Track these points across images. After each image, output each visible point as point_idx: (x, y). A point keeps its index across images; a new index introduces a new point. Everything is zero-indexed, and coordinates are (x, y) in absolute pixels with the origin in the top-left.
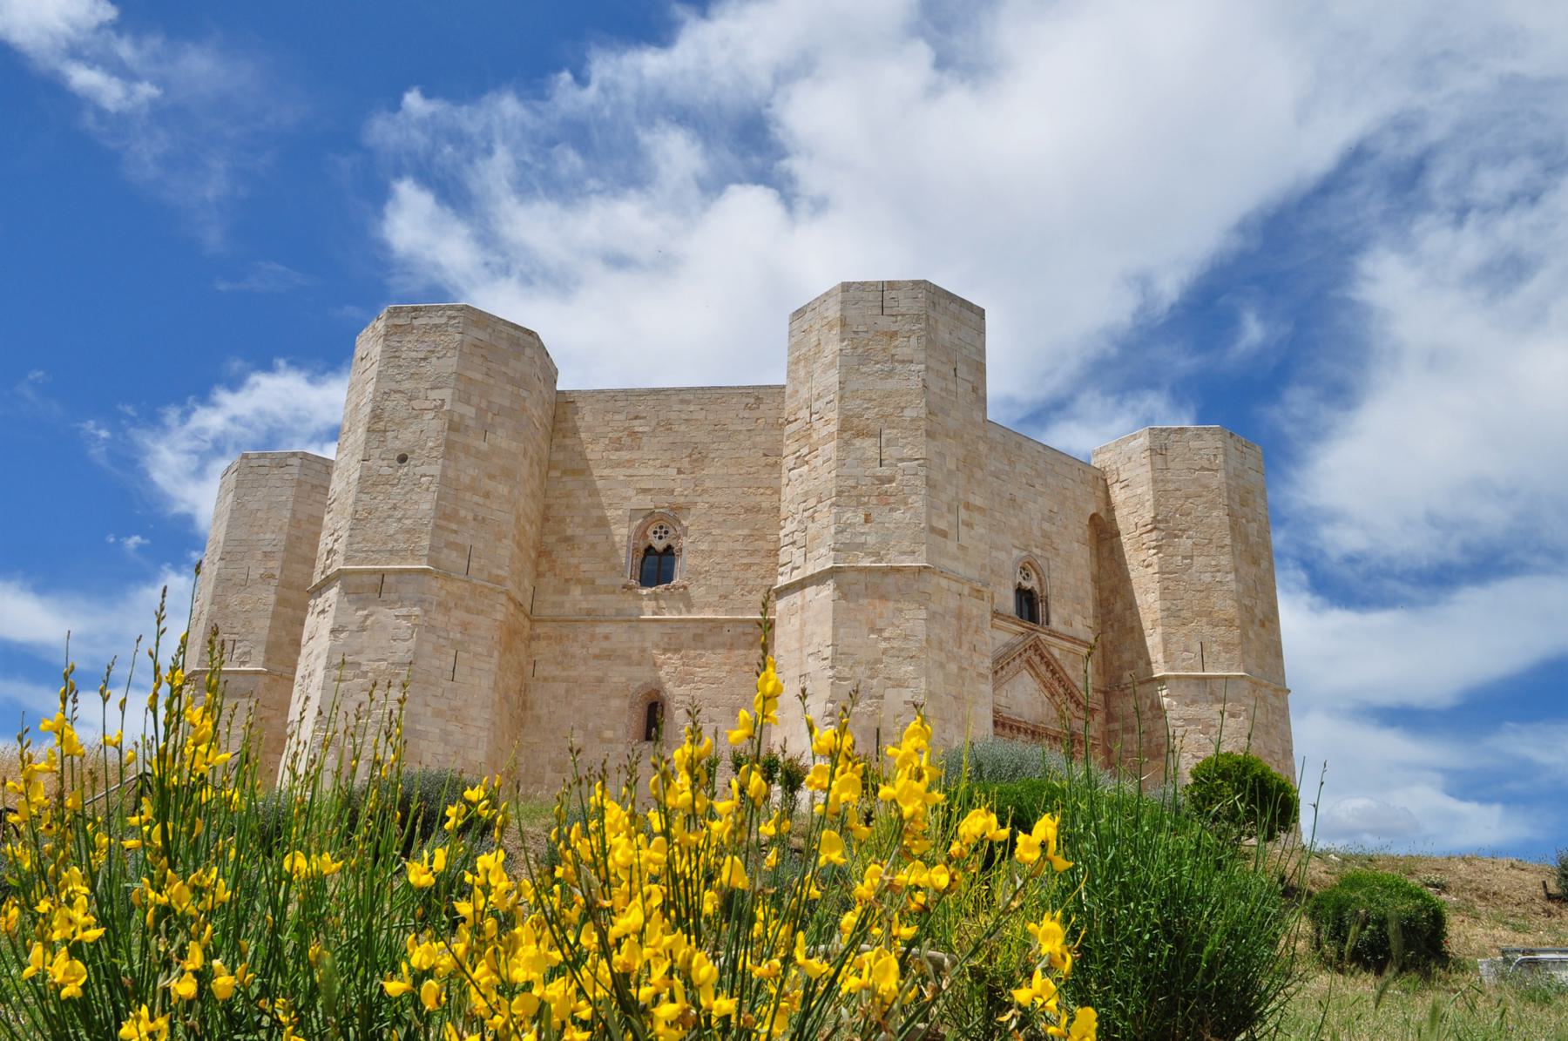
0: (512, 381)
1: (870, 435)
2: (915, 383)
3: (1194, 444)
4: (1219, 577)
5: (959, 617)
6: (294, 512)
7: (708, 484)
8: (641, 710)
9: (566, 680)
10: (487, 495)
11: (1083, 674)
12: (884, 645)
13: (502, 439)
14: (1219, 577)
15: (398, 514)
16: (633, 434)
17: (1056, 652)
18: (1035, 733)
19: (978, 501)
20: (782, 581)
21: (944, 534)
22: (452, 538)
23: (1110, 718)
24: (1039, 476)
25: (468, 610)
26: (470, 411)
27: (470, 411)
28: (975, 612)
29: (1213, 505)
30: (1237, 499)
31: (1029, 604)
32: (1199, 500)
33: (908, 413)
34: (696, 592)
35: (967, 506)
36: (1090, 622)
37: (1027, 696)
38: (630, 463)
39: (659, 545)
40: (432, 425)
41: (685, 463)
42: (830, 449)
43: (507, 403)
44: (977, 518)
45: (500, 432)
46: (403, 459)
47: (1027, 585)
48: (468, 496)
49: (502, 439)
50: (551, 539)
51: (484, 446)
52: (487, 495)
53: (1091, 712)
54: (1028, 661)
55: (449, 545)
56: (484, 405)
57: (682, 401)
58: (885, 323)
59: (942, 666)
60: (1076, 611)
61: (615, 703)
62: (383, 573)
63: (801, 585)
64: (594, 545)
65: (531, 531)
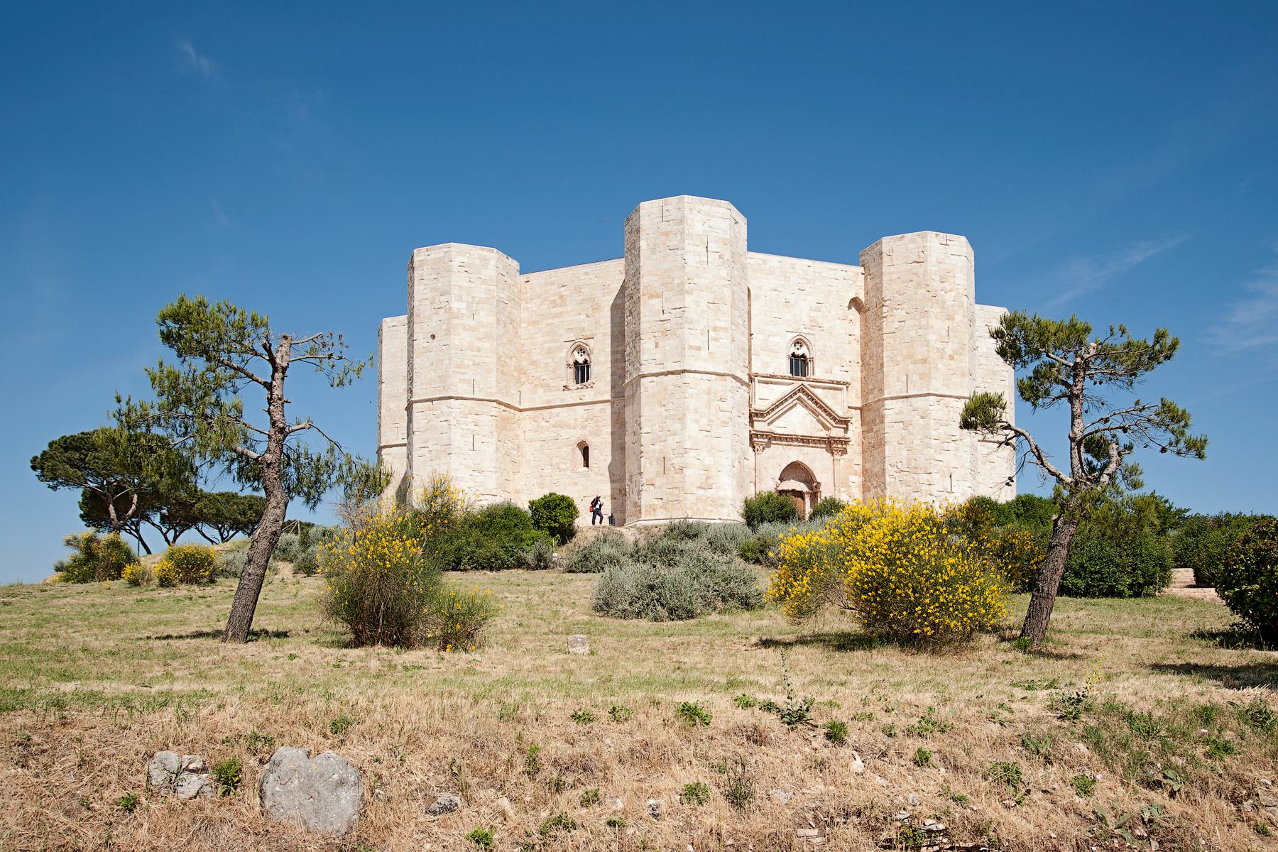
1: (657, 297)
3: (910, 246)
4: (920, 332)
5: (709, 393)
10: (479, 350)
12: (665, 413)
14: (920, 332)
16: (561, 297)
17: (819, 393)
18: (806, 440)
19: (723, 324)
21: (699, 349)
22: (462, 377)
24: (808, 281)
26: (463, 305)
27: (463, 305)
28: (720, 388)
30: (938, 278)
31: (799, 364)
32: (910, 284)
33: (676, 281)
35: (715, 329)
38: (561, 313)
39: (581, 360)
44: (721, 334)
45: (482, 313)
46: (433, 337)
47: (799, 353)
48: (468, 352)
51: (473, 323)
52: (479, 350)
54: (798, 399)
55: (461, 381)
56: (470, 299)
57: (586, 273)
59: (697, 421)
61: (565, 449)
62: (432, 400)
64: (547, 365)
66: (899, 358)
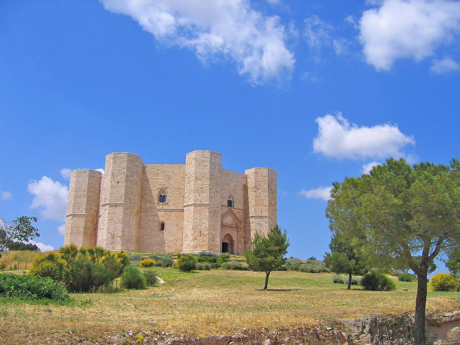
0: (136, 166)
2: (208, 171)
6: (88, 182)
7: (171, 183)
8: (161, 225)
9: (147, 219)
11: (240, 215)
12: (202, 217)
13: (135, 178)
15: (118, 193)
17: (235, 212)
18: (231, 227)
20: (185, 204)
23: (245, 223)
25: (131, 209)
29: (265, 184)
31: (230, 203)
34: (170, 204)
36: (242, 205)
37: (229, 220)
40: (123, 176)
41: (167, 179)
42: (193, 182)
43: (135, 170)
46: (118, 182)
49: (135, 178)
50: (143, 194)
51: (132, 179)
53: (242, 222)
58: (203, 159)
60: (239, 204)
63: (188, 206)
65: (140, 193)
66: (259, 204)
